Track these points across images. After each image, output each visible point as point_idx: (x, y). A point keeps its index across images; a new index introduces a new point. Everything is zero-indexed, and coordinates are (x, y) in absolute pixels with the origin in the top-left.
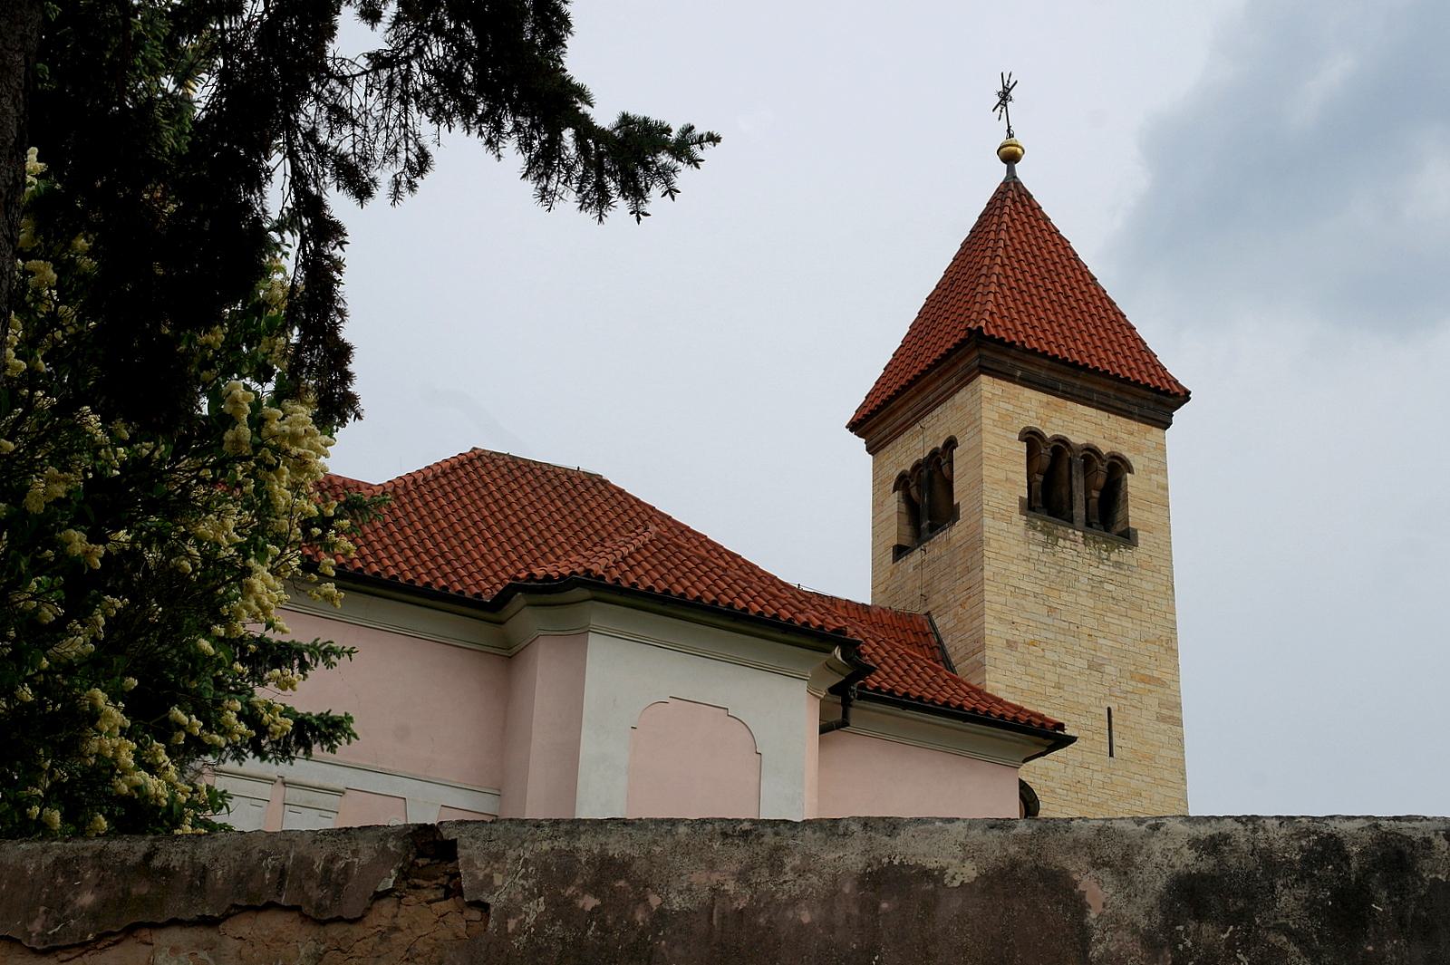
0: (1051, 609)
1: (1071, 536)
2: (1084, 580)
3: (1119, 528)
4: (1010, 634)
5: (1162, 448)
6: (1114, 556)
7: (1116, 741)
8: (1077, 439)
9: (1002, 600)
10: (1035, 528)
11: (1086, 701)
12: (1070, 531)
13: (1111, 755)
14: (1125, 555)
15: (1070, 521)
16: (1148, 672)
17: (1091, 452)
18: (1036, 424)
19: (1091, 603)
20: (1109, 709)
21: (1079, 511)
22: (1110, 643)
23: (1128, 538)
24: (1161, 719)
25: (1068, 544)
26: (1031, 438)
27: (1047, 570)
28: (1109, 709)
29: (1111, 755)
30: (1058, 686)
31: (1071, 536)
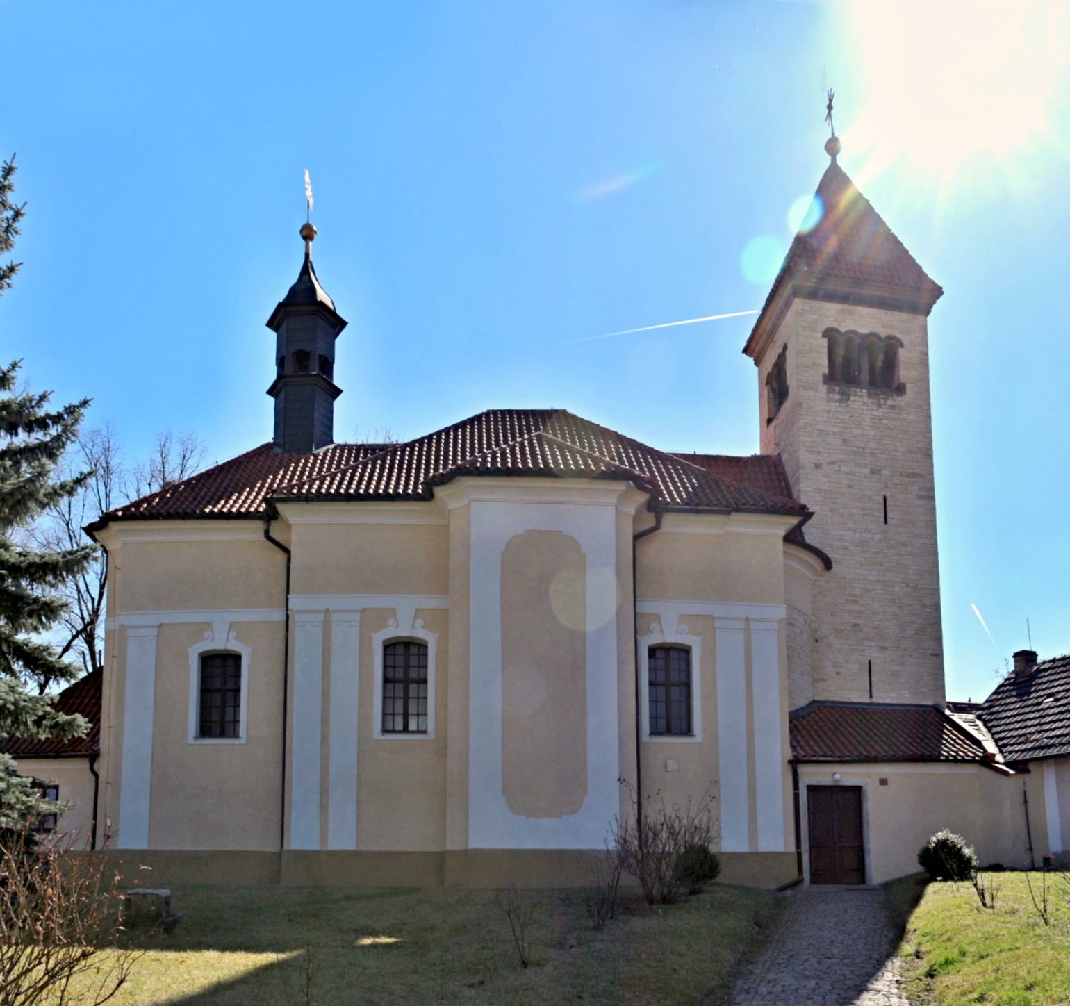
1: (859, 393)
3: (896, 384)
5: (924, 329)
6: (889, 402)
7: (890, 515)
8: (863, 330)
9: (811, 439)
10: (833, 391)
11: (868, 493)
12: (858, 390)
13: (886, 522)
16: (911, 471)
18: (834, 325)
19: (872, 433)
21: (865, 377)
22: (885, 456)
23: (901, 390)
24: (921, 497)
25: (857, 398)
26: (830, 334)
27: (842, 417)
29: (886, 522)
30: (850, 487)
31: (859, 393)
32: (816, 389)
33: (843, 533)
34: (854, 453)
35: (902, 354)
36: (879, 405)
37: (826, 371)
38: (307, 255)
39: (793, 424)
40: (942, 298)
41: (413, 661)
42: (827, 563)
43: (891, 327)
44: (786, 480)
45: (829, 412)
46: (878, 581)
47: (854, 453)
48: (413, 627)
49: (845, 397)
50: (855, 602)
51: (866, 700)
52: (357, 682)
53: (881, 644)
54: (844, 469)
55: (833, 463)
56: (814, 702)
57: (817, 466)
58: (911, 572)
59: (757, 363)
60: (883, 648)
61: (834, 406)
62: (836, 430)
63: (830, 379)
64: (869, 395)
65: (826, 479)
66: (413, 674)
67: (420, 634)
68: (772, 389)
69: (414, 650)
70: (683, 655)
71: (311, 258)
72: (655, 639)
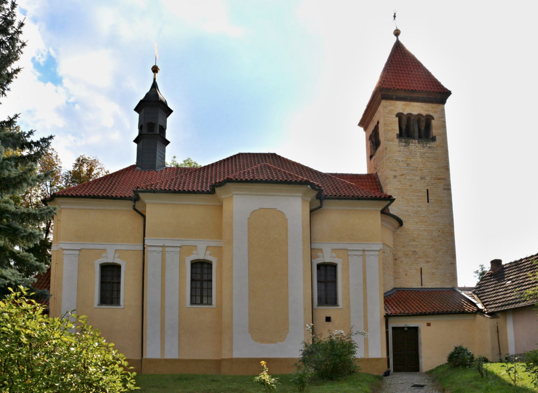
0: (408, 165)
2: (418, 154)
3: (431, 137)
4: (394, 173)
5: (443, 111)
6: (428, 145)
7: (430, 198)
8: (415, 113)
9: (392, 164)
10: (402, 142)
11: (420, 188)
13: (428, 202)
14: (432, 144)
15: (414, 138)
17: (420, 115)
18: (401, 111)
19: (421, 160)
20: (427, 190)
21: (417, 134)
23: (434, 139)
24: (444, 189)
26: (400, 116)
28: (427, 190)
29: (428, 202)
30: (411, 186)
32: (393, 141)
33: (407, 208)
34: (412, 170)
35: (434, 122)
36: (424, 147)
37: (398, 132)
38: (155, 79)
39: (383, 158)
40: (451, 96)
41: (205, 271)
42: (401, 223)
43: (428, 110)
44: (380, 185)
45: (400, 151)
46: (425, 230)
47: (412, 170)
48: (205, 254)
49: (407, 144)
50: (414, 240)
51: (420, 287)
52: (180, 281)
53: (426, 260)
54: (408, 177)
55: (402, 175)
56: (395, 288)
57: (395, 177)
58: (440, 224)
59: (365, 129)
60: (428, 262)
61: (402, 148)
62: (403, 159)
63: (400, 136)
64: (419, 143)
65: (399, 183)
66: (205, 277)
67: (209, 258)
68: (372, 142)
69: (205, 266)
70: (333, 268)
71: (156, 80)
72: (320, 260)
